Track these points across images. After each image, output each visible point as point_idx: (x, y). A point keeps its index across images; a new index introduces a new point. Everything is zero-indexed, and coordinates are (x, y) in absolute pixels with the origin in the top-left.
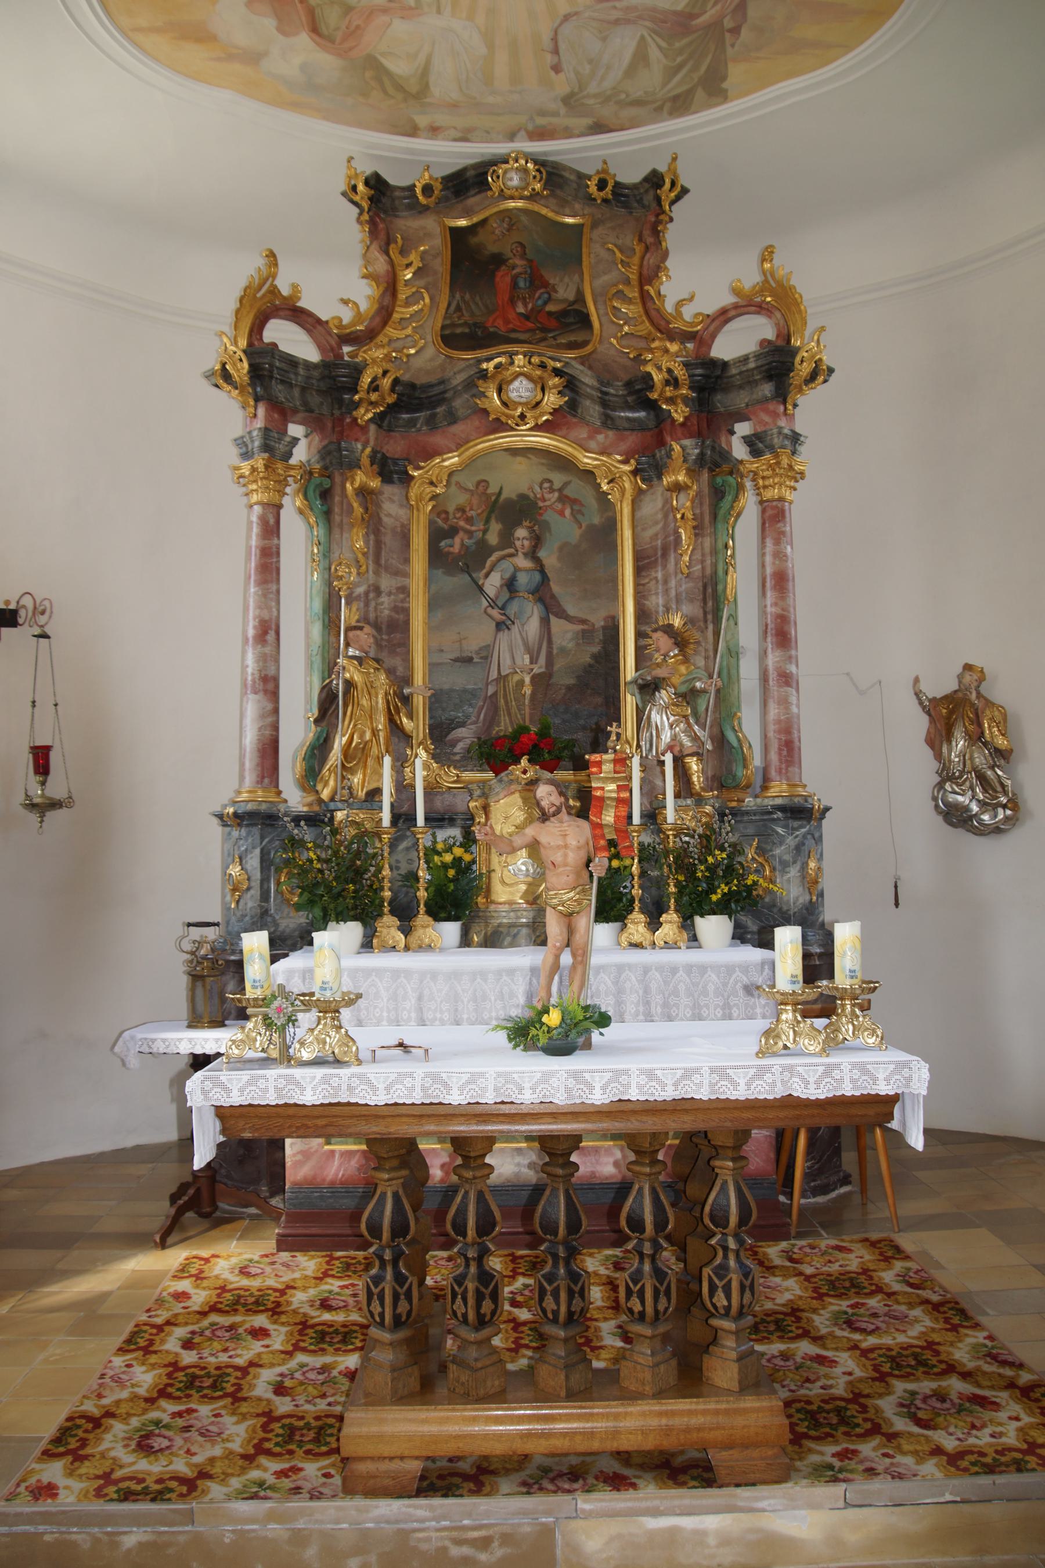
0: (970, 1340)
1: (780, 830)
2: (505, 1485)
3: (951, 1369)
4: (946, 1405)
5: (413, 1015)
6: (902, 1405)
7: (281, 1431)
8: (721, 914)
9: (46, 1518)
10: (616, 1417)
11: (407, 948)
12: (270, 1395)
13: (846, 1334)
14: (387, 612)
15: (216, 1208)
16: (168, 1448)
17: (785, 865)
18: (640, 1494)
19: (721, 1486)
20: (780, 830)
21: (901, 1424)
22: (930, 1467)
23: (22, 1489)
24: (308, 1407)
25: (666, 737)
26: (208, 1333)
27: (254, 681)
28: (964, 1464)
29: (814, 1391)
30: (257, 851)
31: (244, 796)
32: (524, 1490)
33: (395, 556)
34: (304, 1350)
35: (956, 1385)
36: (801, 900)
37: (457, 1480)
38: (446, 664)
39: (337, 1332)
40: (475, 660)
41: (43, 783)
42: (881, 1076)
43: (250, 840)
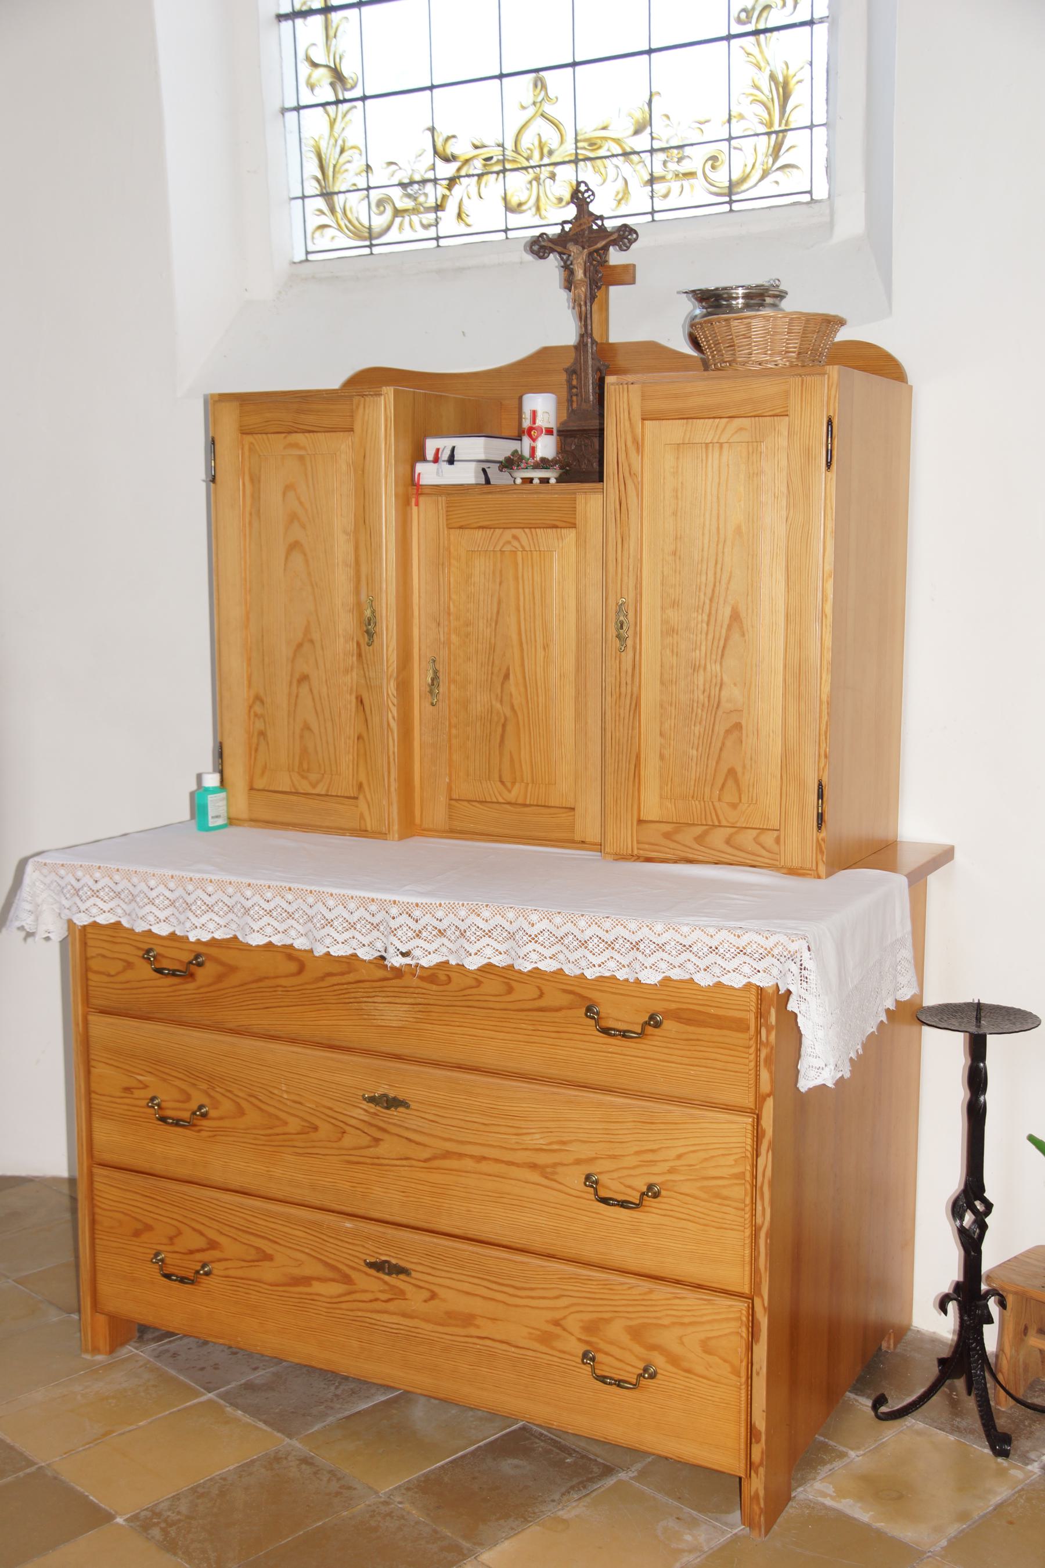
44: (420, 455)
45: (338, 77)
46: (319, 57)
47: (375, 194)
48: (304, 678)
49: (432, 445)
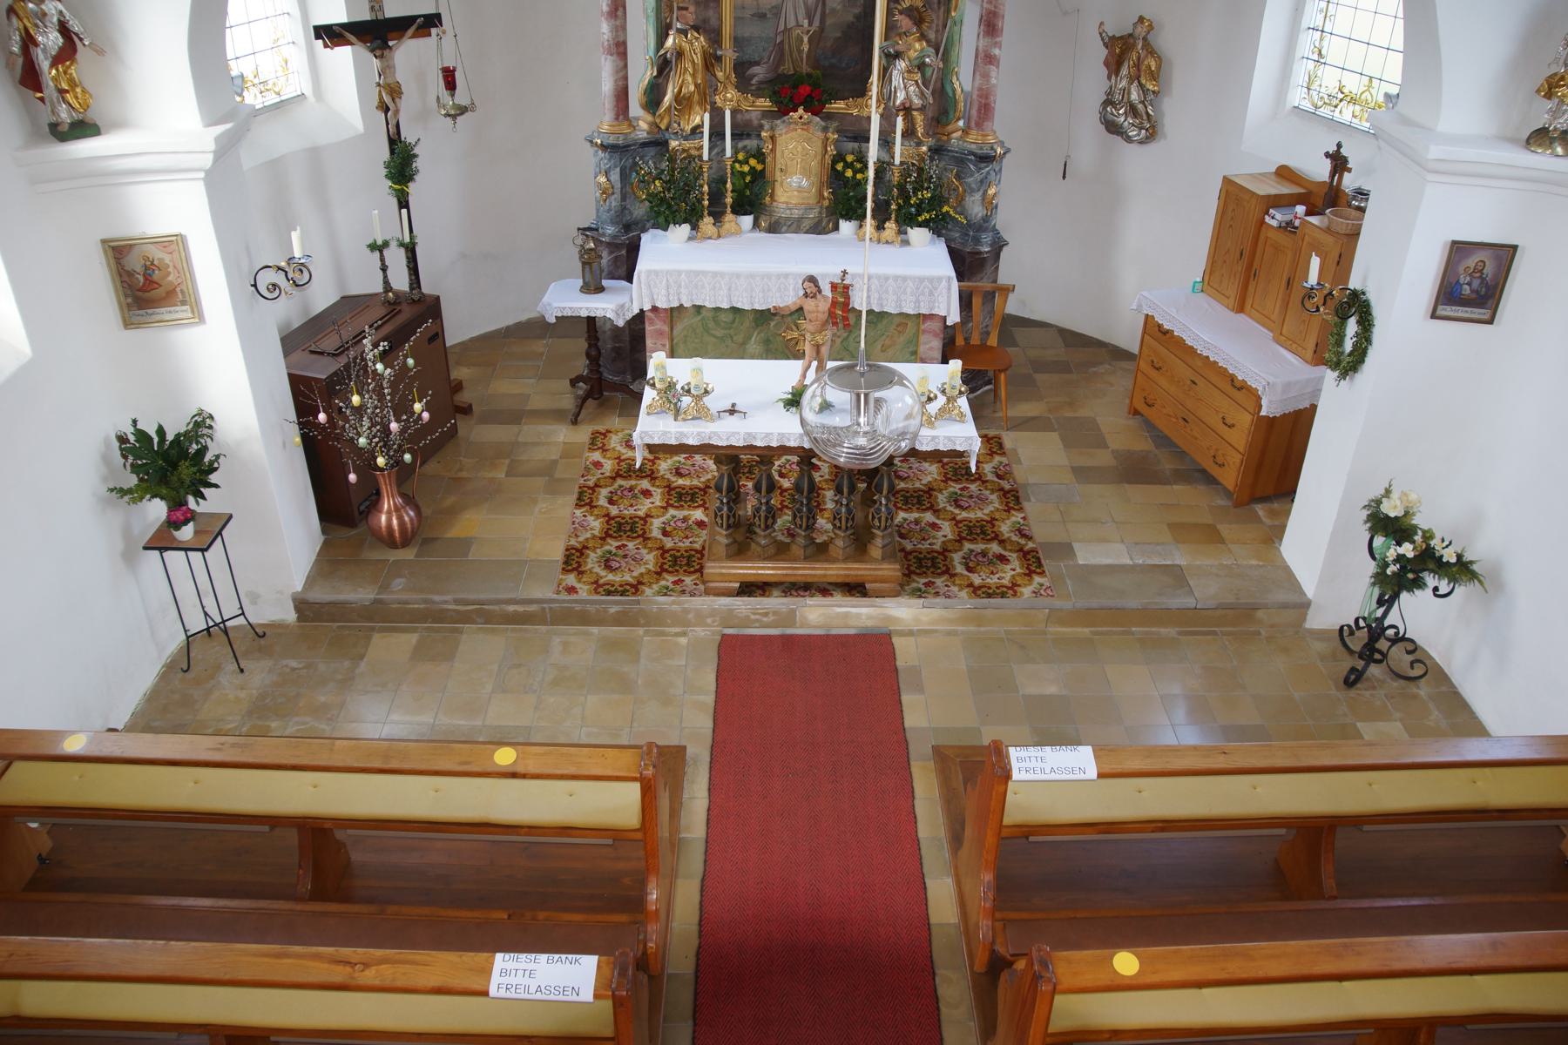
0: (1013, 519)
1: (972, 167)
2: (776, 593)
3: (997, 538)
4: (985, 560)
5: (725, 299)
6: (964, 558)
7: (670, 559)
8: (924, 227)
9: (576, 601)
10: (826, 569)
11: (719, 236)
12: (660, 536)
13: (952, 509)
15: (602, 394)
16: (620, 567)
17: (972, 191)
18: (834, 599)
19: (870, 597)
20: (972, 167)
21: (960, 569)
22: (964, 594)
23: (561, 589)
24: (681, 544)
25: (901, 96)
26: (619, 493)
27: (609, 45)
28: (979, 592)
29: (925, 546)
30: (618, 169)
31: (605, 128)
32: (783, 594)
34: (672, 506)
35: (995, 548)
36: (980, 215)
37: (754, 588)
39: (687, 493)
40: (768, 16)
41: (453, 95)
42: (958, 442)
43: (612, 162)
44: (1267, 213)
45: (1320, 53)
46: (1317, 44)
47: (1321, 95)
48: (1225, 262)
49: (1271, 211)
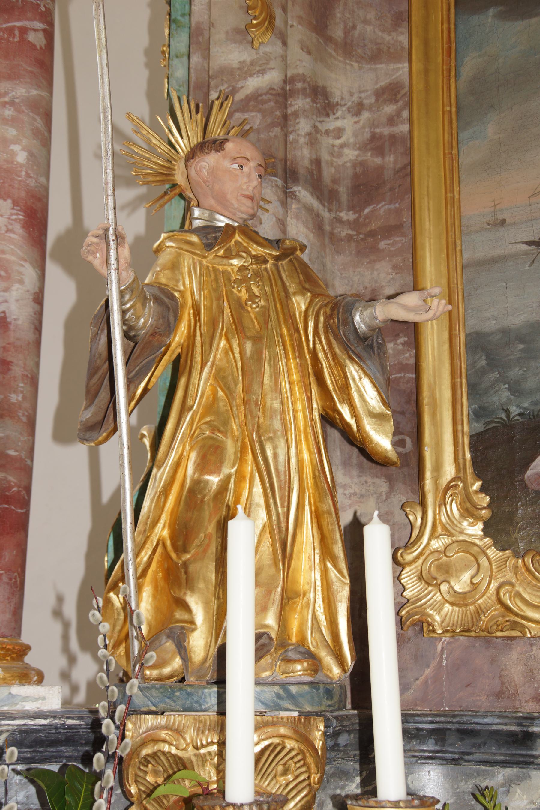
14: (350, 154)
33: (371, 16)
38: (515, 256)
